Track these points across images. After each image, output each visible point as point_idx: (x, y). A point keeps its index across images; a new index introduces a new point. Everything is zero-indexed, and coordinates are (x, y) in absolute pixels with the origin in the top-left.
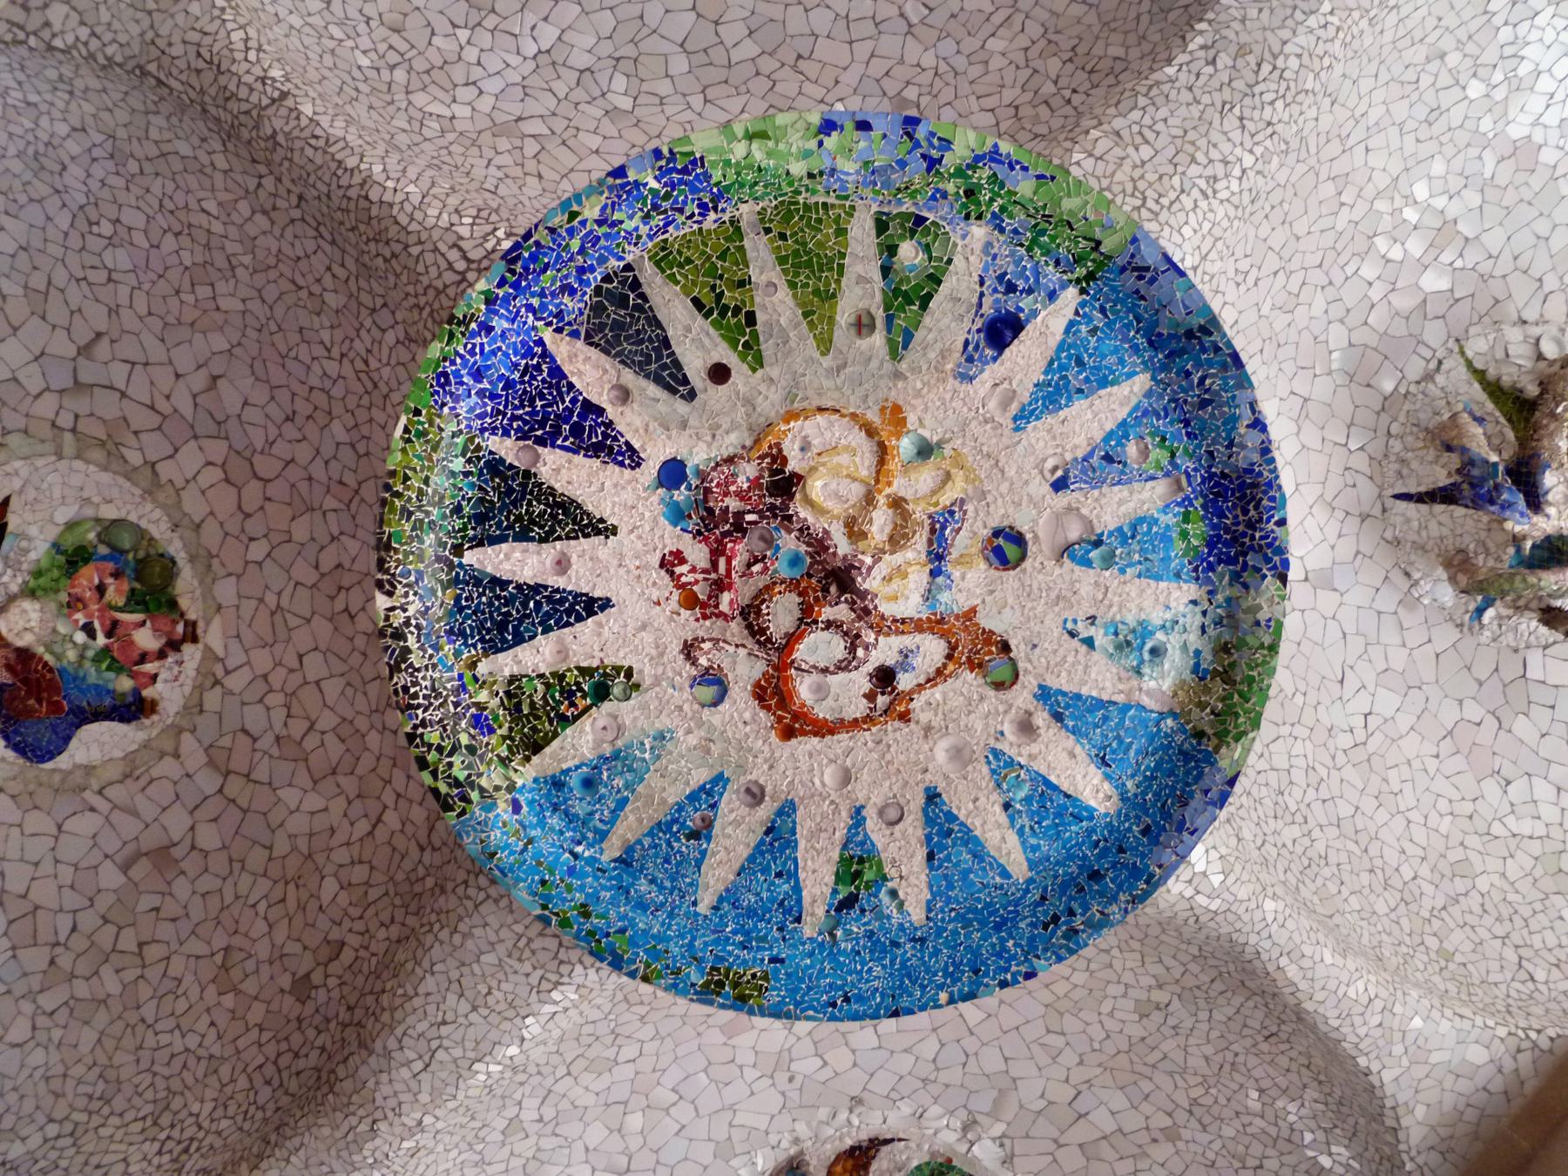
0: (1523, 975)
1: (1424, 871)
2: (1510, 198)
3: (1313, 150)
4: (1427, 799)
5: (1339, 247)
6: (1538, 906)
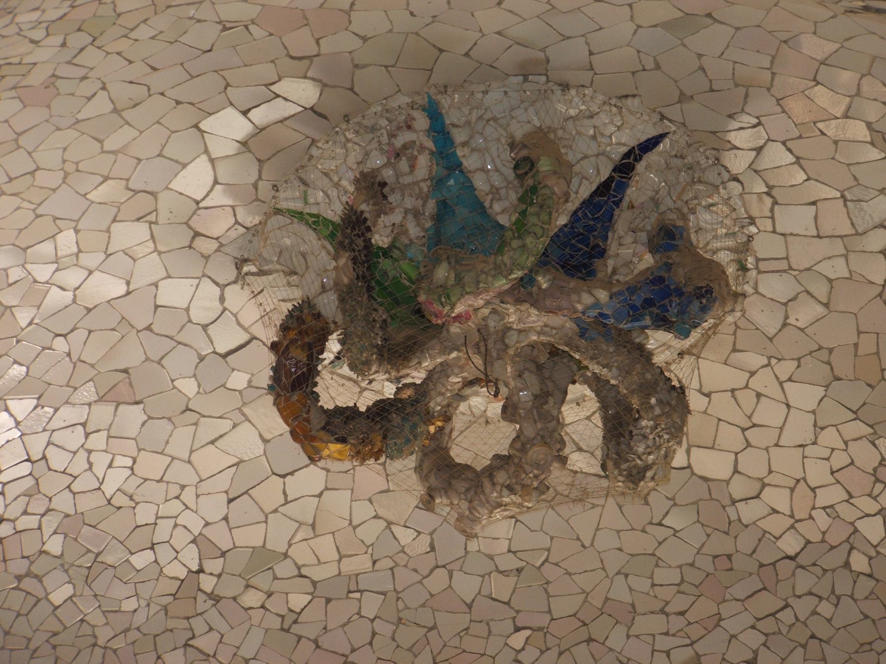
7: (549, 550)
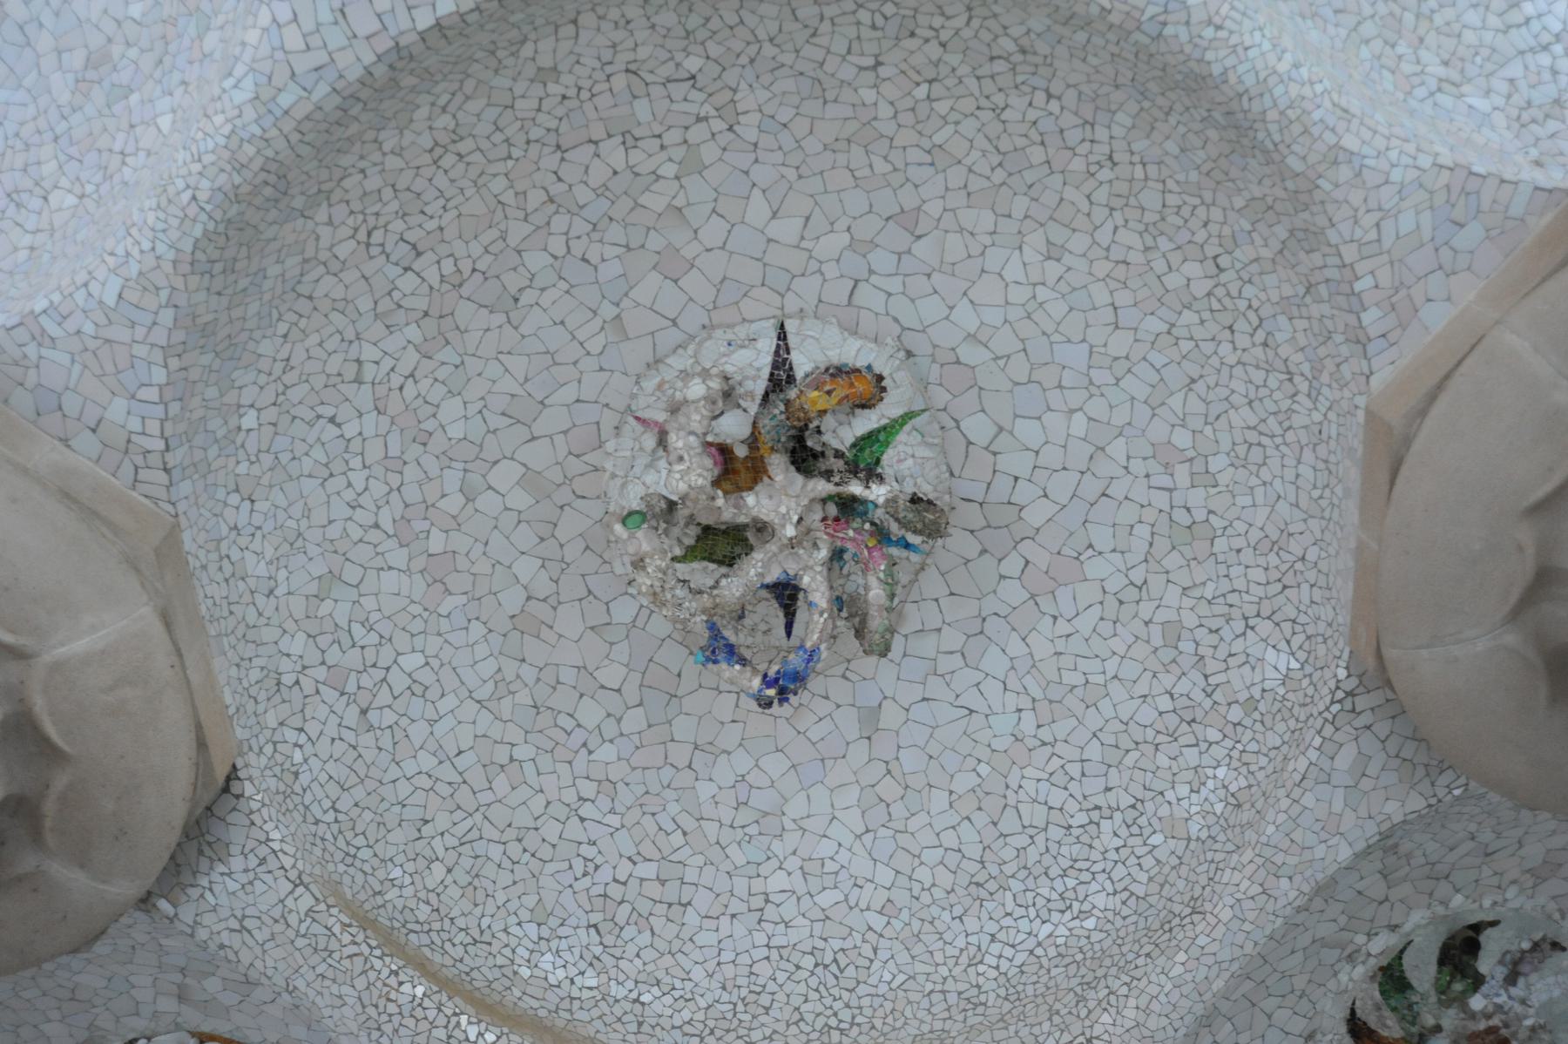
0: (1287, 627)
1: (1167, 680)
2: (483, 567)
3: (469, 822)
4: (1097, 645)
5: (549, 745)
6: (1222, 570)
7: (516, 328)
